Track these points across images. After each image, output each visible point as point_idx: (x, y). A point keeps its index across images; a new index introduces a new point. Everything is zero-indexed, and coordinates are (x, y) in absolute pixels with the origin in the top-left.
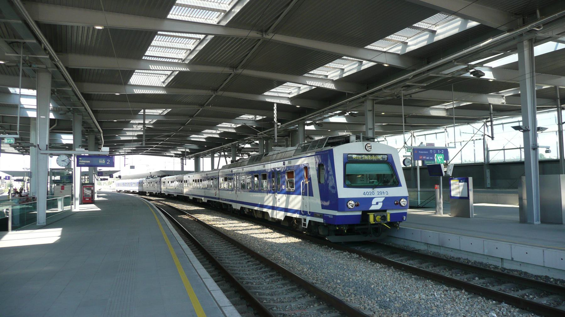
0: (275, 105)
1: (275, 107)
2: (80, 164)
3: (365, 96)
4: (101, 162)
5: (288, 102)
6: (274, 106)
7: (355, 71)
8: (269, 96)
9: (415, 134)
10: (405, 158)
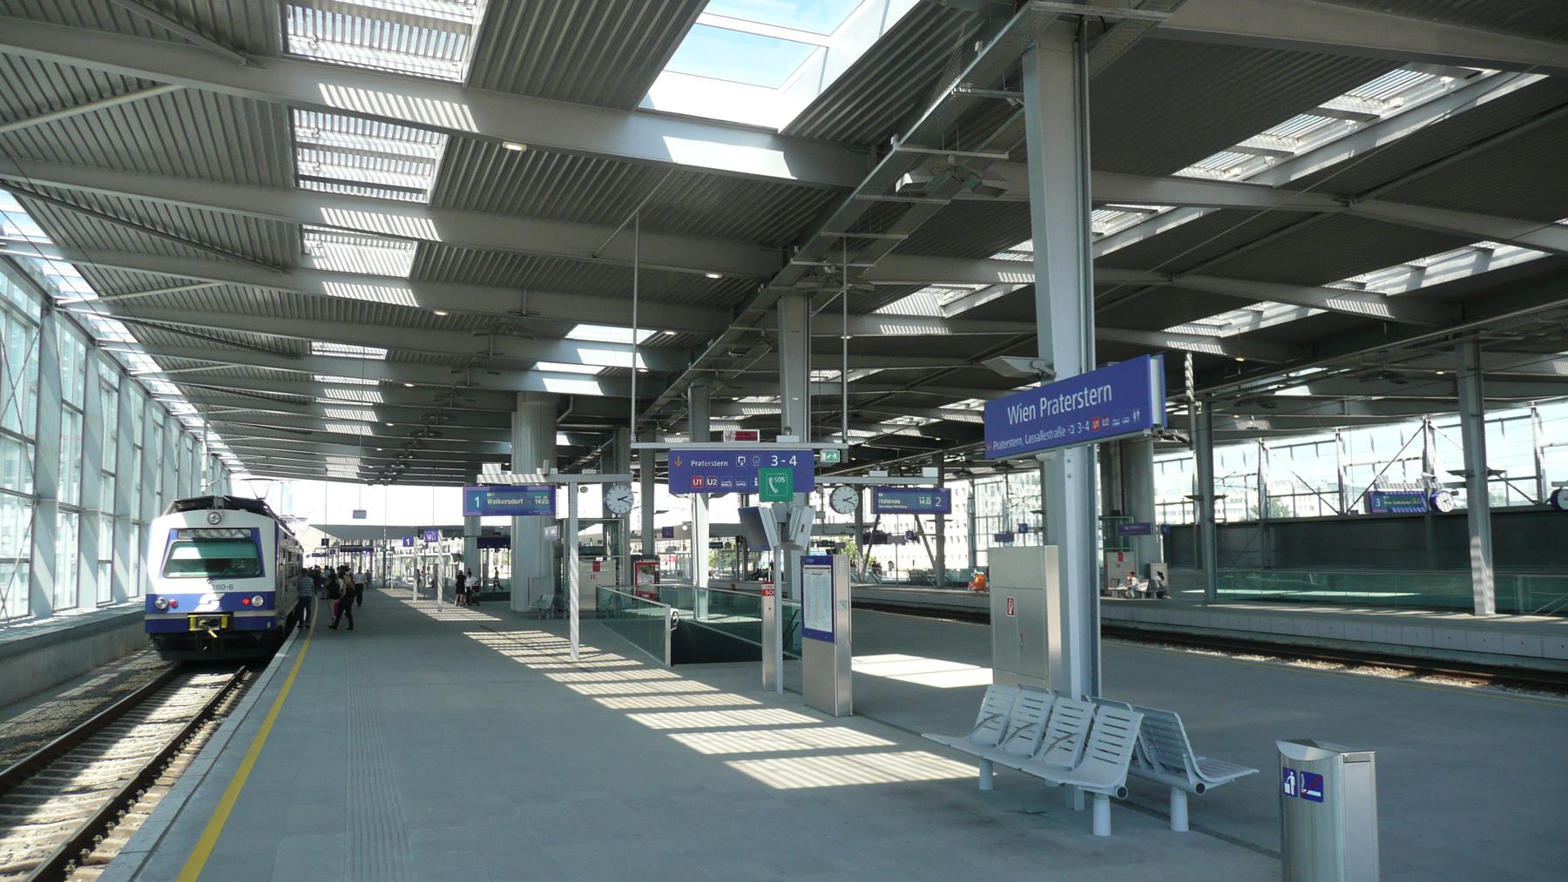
0: (1189, 356)
1: (1189, 363)
2: (880, 506)
3: (1456, 335)
5: (1216, 350)
6: (1185, 359)
7: (1467, 273)
8: (1189, 335)
9: (1435, 423)
10: (1558, 488)
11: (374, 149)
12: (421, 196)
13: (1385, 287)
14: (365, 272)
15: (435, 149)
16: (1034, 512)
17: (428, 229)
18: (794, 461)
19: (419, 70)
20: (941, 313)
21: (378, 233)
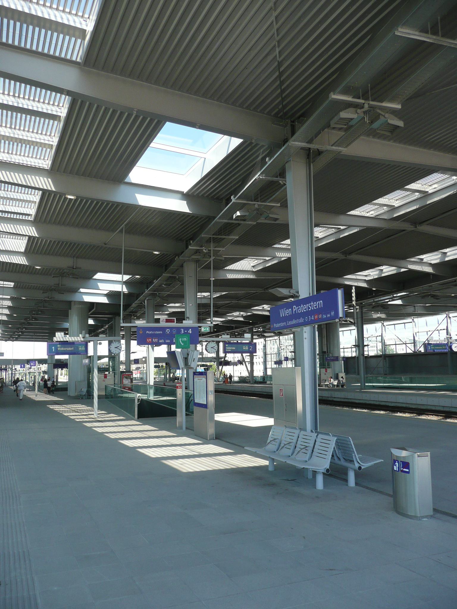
0: (354, 288)
1: (353, 290)
2: (227, 350)
4: (245, 348)
5: (364, 285)
6: (352, 289)
9: (451, 315)
11: (9, 196)
12: (30, 217)
13: (431, 260)
14: (4, 249)
15: (36, 197)
16: (291, 352)
17: (32, 231)
18: (190, 331)
19: (29, 163)
20: (252, 269)
21: (10, 233)
